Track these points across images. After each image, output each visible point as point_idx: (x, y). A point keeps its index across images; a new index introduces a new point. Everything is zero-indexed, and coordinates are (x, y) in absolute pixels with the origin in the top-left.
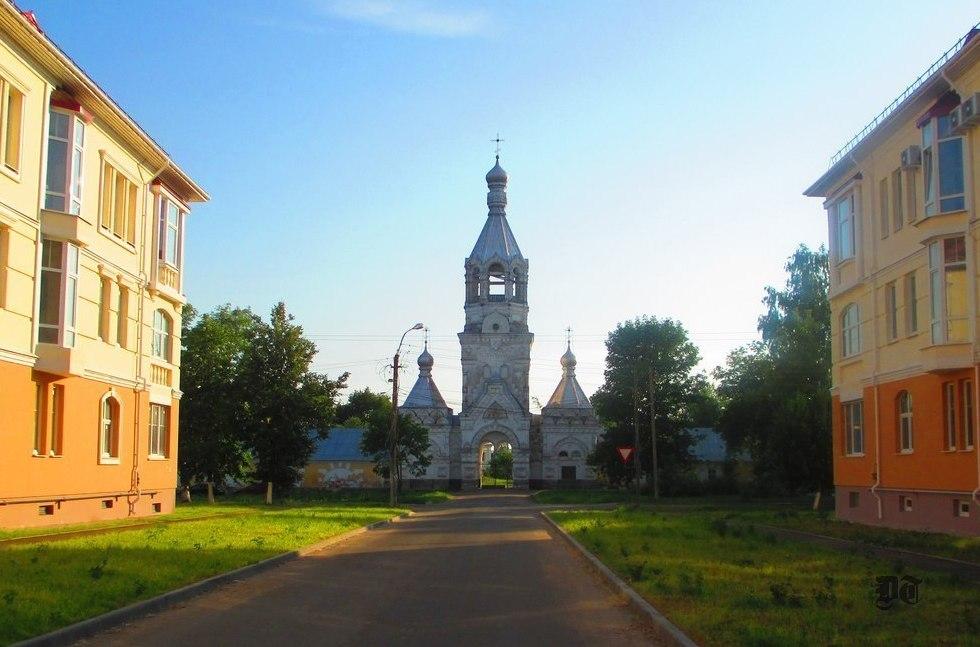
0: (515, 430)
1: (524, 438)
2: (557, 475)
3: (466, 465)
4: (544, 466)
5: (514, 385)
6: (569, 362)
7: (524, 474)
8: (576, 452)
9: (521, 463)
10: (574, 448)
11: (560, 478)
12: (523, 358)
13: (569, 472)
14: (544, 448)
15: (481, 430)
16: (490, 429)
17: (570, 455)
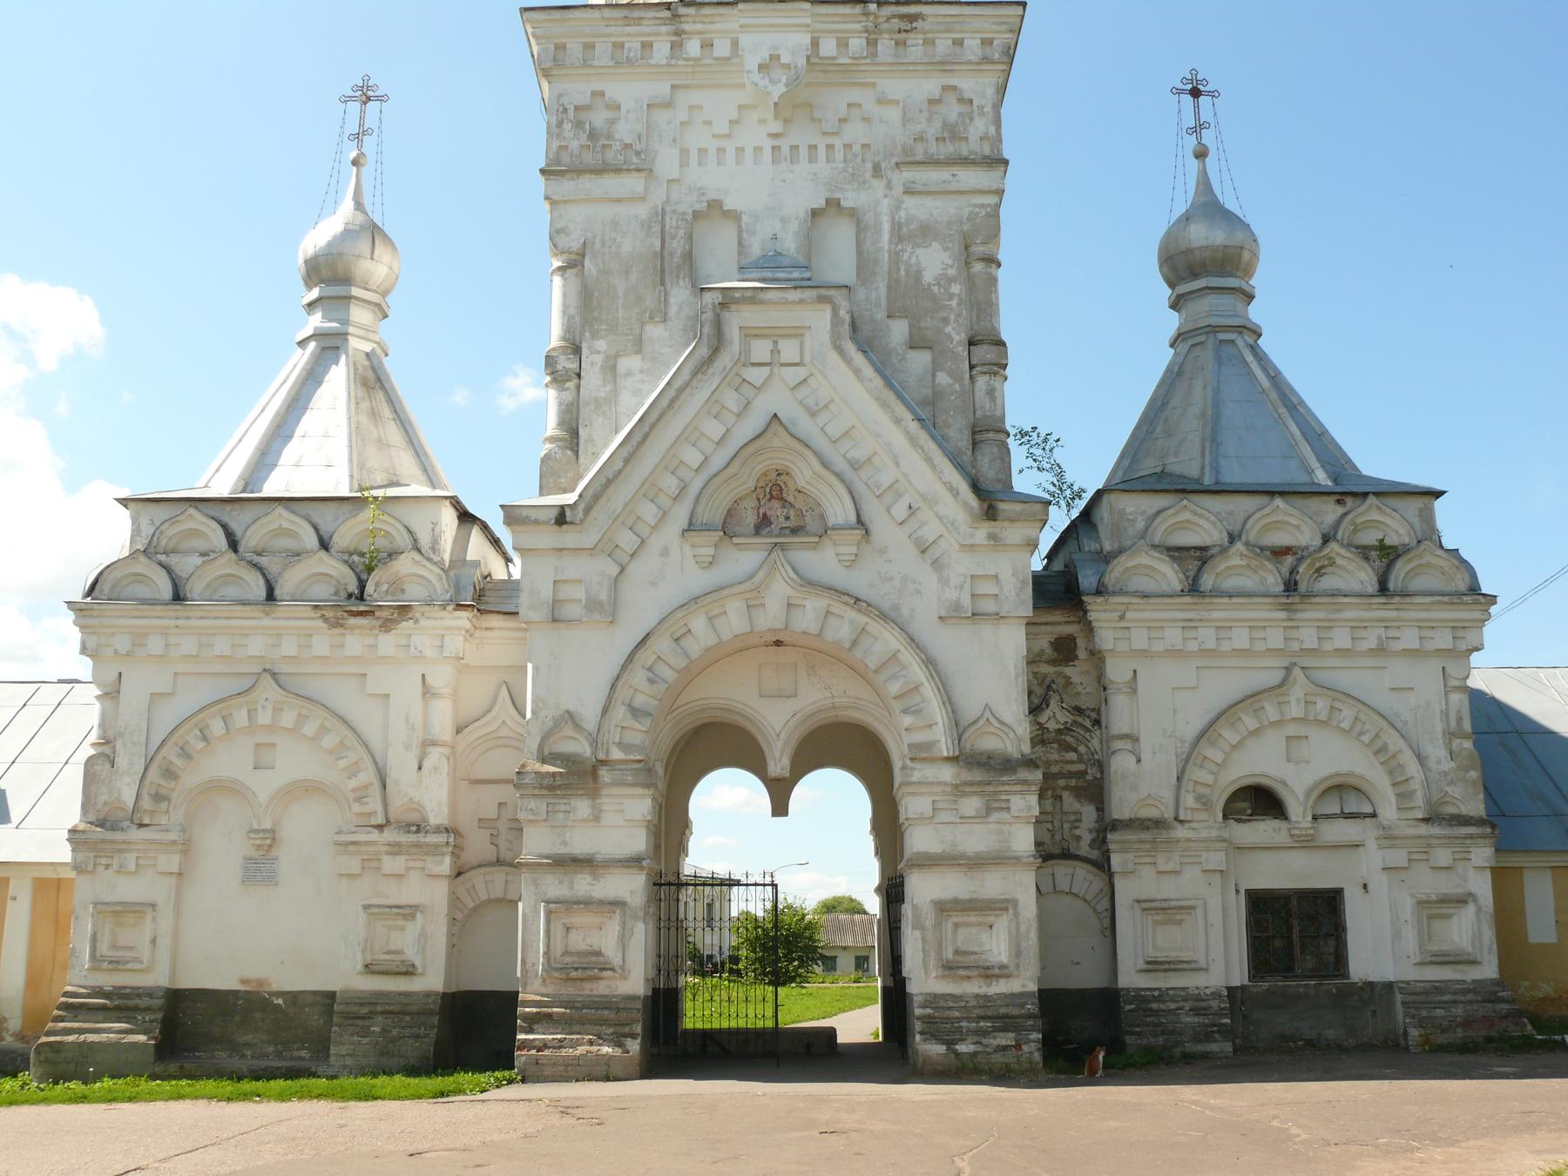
0: (923, 612)
1: (992, 673)
2: (1218, 957)
3: (555, 886)
4: (1126, 890)
5: (898, 331)
6: (1206, 269)
7: (996, 945)
8: (1339, 788)
9: (975, 863)
10: (1332, 756)
11: (1239, 975)
13: (1294, 927)
14: (1121, 764)
15: (672, 621)
16: (734, 621)
17: (1297, 809)
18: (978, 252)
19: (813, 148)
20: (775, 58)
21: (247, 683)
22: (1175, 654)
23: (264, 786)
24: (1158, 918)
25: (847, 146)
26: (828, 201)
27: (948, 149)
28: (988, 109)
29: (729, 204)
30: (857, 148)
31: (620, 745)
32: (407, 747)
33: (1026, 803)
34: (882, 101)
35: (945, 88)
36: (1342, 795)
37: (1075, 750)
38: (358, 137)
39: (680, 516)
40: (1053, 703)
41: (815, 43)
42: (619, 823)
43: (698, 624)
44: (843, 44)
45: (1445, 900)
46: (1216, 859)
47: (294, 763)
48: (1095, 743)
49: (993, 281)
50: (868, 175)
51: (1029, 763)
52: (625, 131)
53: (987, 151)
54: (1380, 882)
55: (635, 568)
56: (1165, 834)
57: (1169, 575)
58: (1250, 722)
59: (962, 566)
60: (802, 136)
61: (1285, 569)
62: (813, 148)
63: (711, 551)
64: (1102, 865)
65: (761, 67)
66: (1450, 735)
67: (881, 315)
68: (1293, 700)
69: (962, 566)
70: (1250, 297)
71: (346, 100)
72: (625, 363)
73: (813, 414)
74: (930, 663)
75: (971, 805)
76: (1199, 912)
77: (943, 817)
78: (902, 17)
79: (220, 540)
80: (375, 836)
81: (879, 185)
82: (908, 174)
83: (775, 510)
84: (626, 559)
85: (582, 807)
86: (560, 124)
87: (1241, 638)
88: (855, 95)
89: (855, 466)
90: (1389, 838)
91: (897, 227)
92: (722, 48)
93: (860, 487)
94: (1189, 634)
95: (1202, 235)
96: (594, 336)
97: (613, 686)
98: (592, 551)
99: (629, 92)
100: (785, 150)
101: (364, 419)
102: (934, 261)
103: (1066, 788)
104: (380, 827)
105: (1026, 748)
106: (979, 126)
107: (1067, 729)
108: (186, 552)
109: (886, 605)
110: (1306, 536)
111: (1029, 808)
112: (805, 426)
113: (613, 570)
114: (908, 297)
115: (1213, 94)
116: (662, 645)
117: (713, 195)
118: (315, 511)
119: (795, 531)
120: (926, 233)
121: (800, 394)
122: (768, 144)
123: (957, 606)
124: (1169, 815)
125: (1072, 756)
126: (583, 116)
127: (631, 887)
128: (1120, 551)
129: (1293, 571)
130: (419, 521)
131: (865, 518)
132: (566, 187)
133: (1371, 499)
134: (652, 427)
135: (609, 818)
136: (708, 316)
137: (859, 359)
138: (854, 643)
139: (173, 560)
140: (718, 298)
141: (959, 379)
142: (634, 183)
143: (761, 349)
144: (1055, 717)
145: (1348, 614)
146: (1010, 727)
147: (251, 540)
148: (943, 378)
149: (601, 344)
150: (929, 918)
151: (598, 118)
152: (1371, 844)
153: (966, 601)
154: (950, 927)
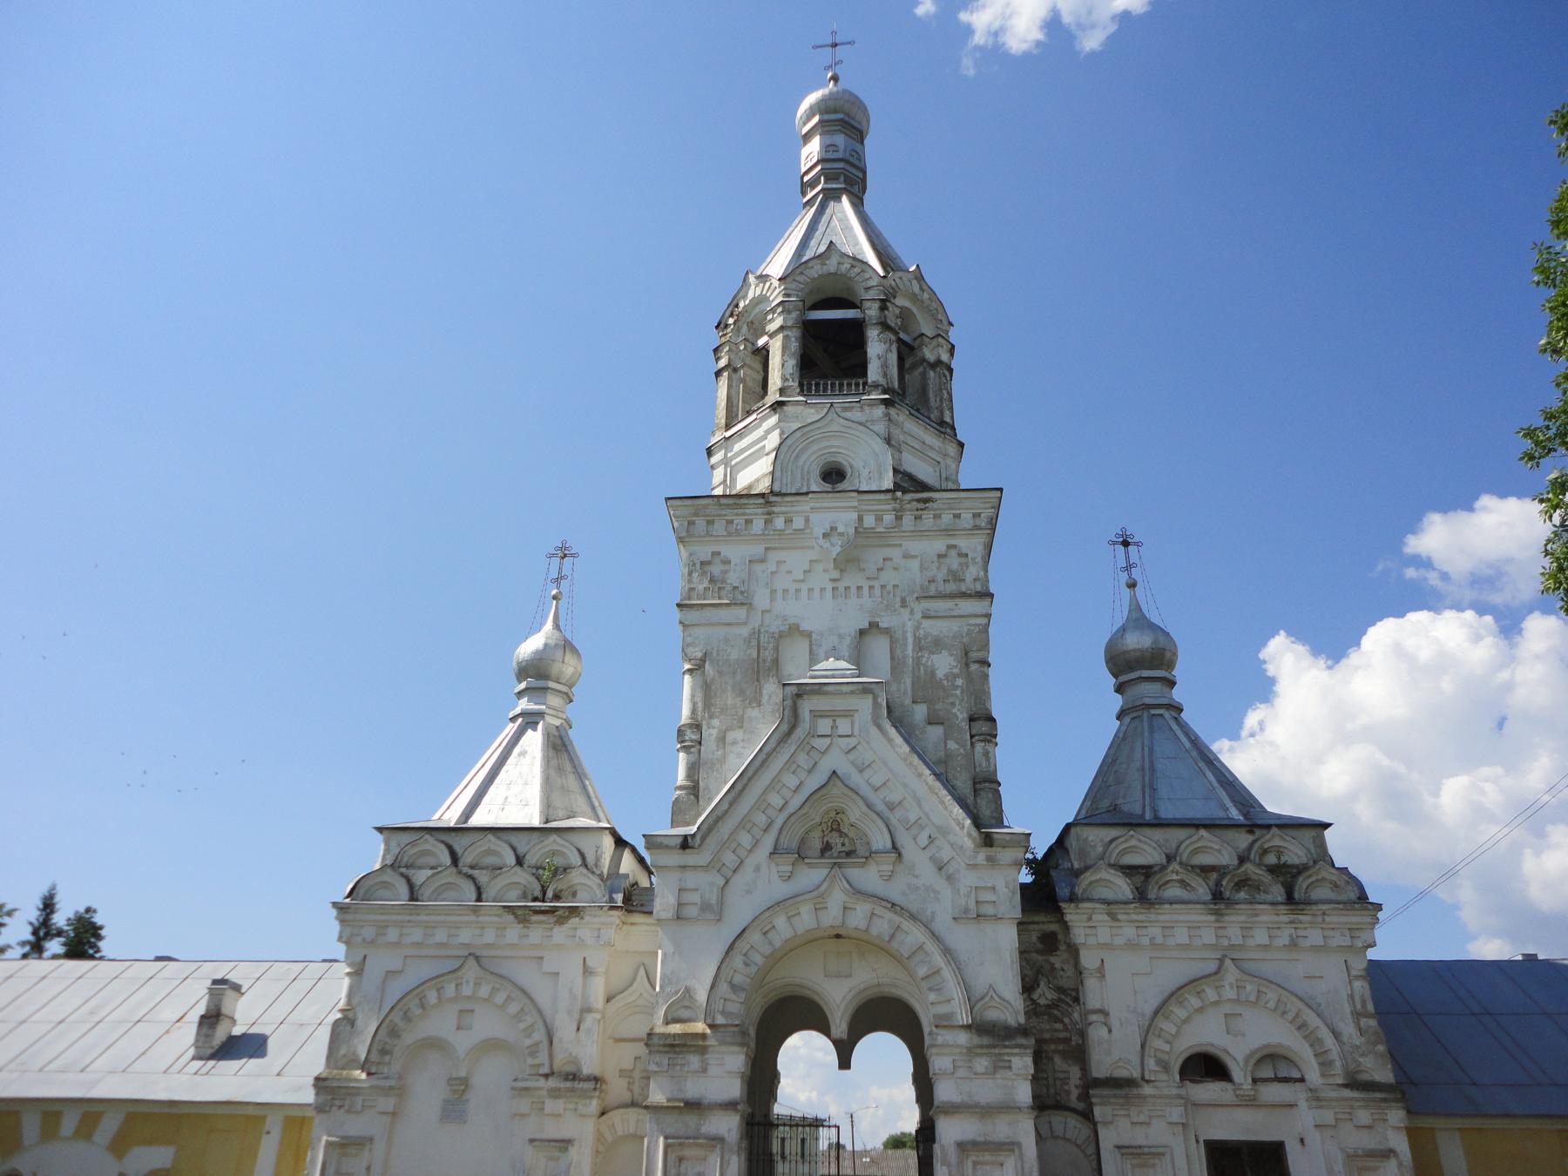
0: (943, 911)
1: (994, 961)
4: (1108, 1139)
5: (920, 712)
6: (1141, 667)
8: (1271, 1057)
9: (987, 1111)
14: (1097, 1033)
16: (806, 919)
18: (975, 659)
19: (859, 588)
20: (833, 529)
21: (457, 964)
22: (1131, 946)
23: (463, 1042)
24: (1136, 1161)
25: (883, 587)
26: (871, 624)
27: (951, 587)
28: (979, 560)
29: (805, 626)
30: (890, 588)
31: (723, 1013)
32: (569, 1012)
33: (1023, 1063)
34: (906, 556)
35: (949, 547)
36: (1274, 1065)
37: (1061, 1021)
38: (557, 581)
39: (768, 843)
40: (1042, 984)
41: (860, 519)
42: (723, 1077)
43: (780, 922)
44: (879, 519)
45: (1371, 1154)
46: (1176, 1114)
47: (487, 1025)
48: (1076, 1015)
49: (986, 676)
50: (898, 605)
51: (1023, 1031)
52: (733, 579)
53: (979, 588)
54: (1314, 1137)
55: (738, 882)
56: (1135, 1091)
57: (1122, 887)
58: (1194, 1002)
59: (968, 879)
60: (853, 580)
61: (1211, 883)
62: (859, 588)
63: (790, 868)
64: (1087, 1115)
65: (825, 535)
66: (1357, 1015)
67: (908, 701)
68: (1226, 983)
69: (968, 879)
70: (1171, 683)
71: (551, 556)
72: (731, 736)
73: (861, 771)
74: (947, 951)
75: (982, 1064)
76: (1168, 1157)
77: (961, 1073)
78: (918, 501)
79: (446, 859)
80: (542, 1082)
81: (905, 612)
82: (925, 604)
83: (835, 839)
84: (729, 874)
85: (694, 1060)
86: (690, 574)
87: (1181, 936)
88: (888, 552)
89: (891, 807)
90: (1316, 1099)
91: (917, 640)
92: (798, 523)
93: (894, 821)
94: (1141, 932)
95: (1137, 641)
96: (711, 717)
98: (706, 868)
99: (737, 552)
100: (842, 589)
101: (552, 772)
102: (944, 664)
103: (1055, 1051)
104: (546, 1076)
105: (1022, 1020)
106: (973, 571)
107: (1054, 1005)
108: (420, 868)
109: (914, 906)
110: (1226, 858)
111: (1026, 1067)
112: (856, 779)
113: (721, 882)
114: (927, 688)
115: (1137, 544)
116: (755, 937)
117: (792, 620)
118: (514, 839)
119: (849, 854)
120: (938, 644)
121: (851, 756)
122: (829, 586)
123: (966, 910)
124: (1136, 1074)
125: (1059, 1026)
126: (707, 568)
127: (728, 1126)
128: (1087, 868)
129: (1218, 883)
130: (586, 843)
131: (899, 845)
132: (693, 616)
133: (1274, 830)
134: (750, 779)
135: (713, 1070)
136: (789, 702)
137: (892, 732)
138: (892, 936)
139: (411, 872)
140: (794, 690)
141: (963, 746)
142: (741, 613)
143: (824, 726)
144: (1045, 994)
145: (1264, 918)
146: (1010, 1005)
147: (467, 859)
148: (952, 745)
149: (716, 722)
150: (953, 1159)
151: (716, 569)
152: (1303, 1104)
153: (972, 905)
154: (970, 1164)
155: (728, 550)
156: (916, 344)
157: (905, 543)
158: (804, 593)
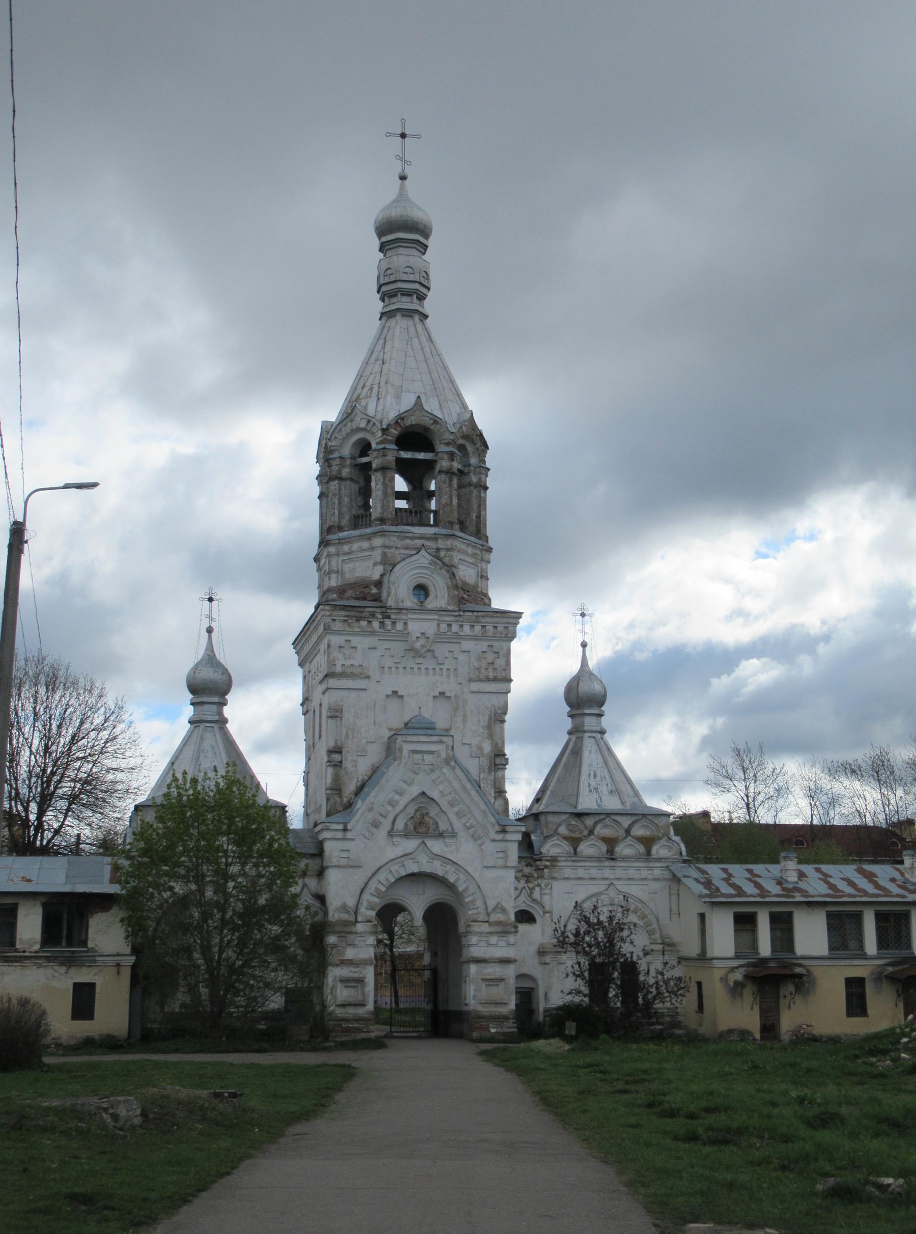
12: (495, 679)
39: (387, 823)
44: (449, 625)
92: (400, 626)
97: (361, 893)
155: (355, 640)
156: (466, 471)
157: (463, 642)
158: (401, 670)
